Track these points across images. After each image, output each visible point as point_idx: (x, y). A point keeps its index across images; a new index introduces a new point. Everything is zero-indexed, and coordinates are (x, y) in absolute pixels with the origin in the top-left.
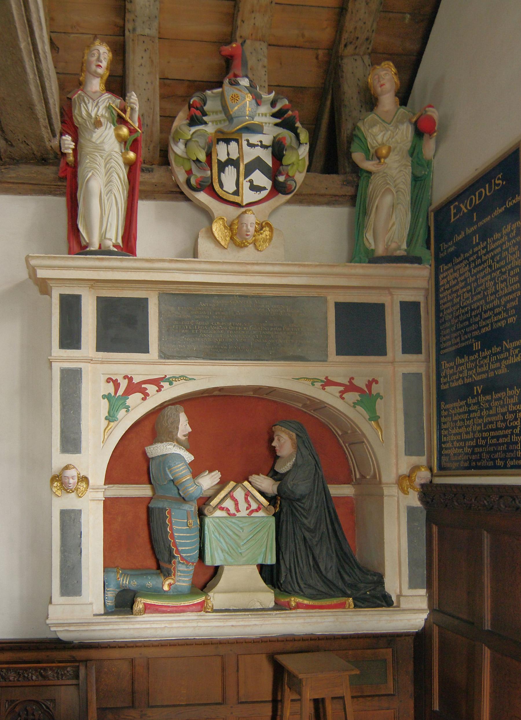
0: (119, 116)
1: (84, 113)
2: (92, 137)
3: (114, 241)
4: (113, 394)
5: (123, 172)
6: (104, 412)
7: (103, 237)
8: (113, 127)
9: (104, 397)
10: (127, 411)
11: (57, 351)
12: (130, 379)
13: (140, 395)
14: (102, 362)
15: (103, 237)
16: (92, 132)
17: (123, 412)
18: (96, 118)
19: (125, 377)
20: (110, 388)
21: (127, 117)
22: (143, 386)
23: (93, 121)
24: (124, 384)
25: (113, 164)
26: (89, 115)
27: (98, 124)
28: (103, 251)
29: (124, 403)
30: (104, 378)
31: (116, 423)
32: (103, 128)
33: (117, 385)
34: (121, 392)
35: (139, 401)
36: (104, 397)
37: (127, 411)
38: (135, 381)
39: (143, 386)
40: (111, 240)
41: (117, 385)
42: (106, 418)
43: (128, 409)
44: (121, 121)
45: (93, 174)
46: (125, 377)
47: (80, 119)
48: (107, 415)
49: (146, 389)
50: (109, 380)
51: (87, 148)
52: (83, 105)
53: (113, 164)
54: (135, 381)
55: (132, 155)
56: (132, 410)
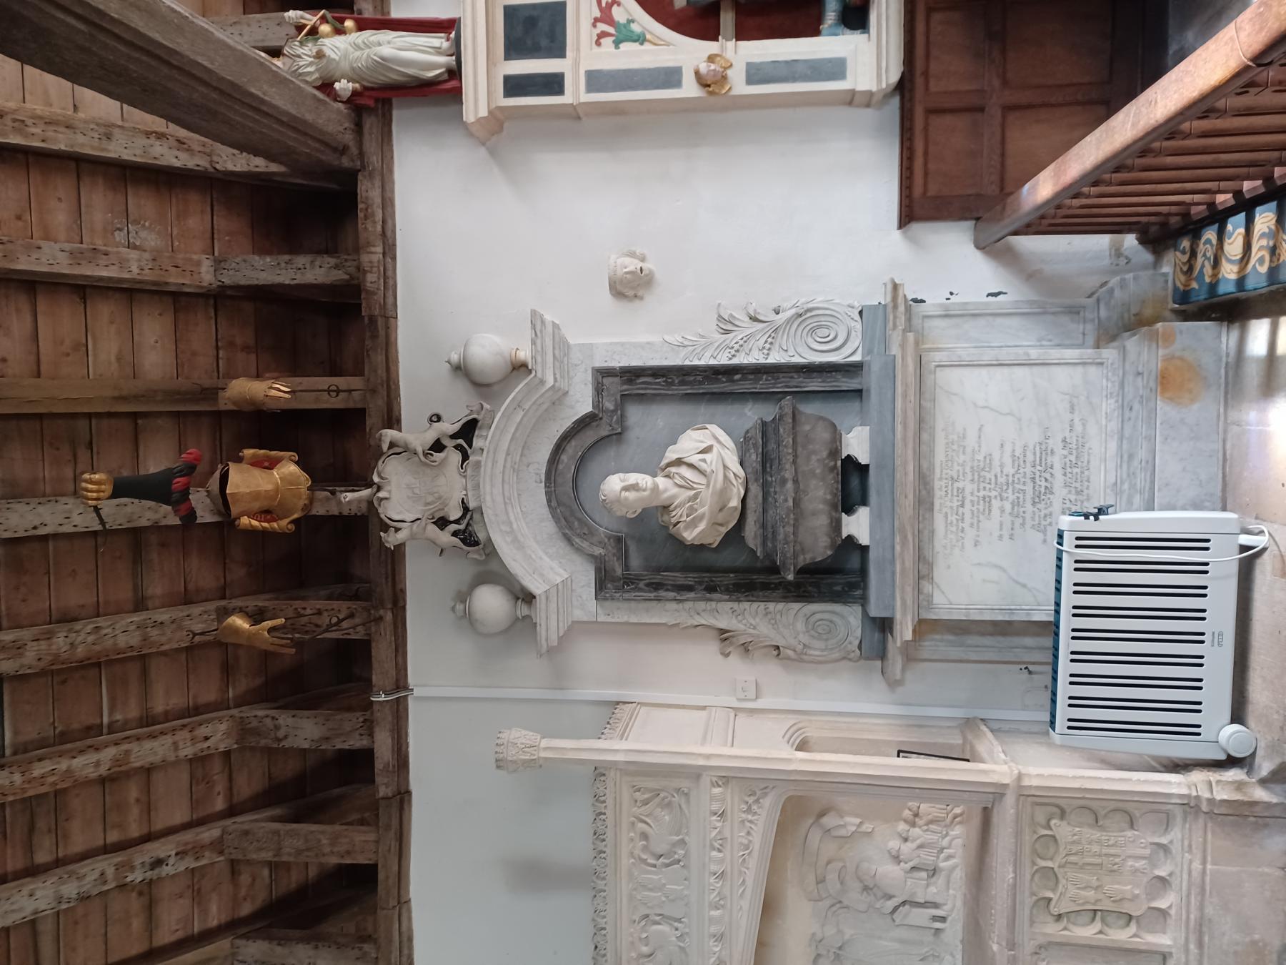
0: (307, 34)
1: (309, 69)
2: (334, 60)
3: (443, 40)
4: (614, 38)
5: (368, 35)
6: (634, 46)
7: (438, 51)
8: (321, 40)
9: (617, 47)
10: (633, 21)
11: (566, 99)
12: (596, 20)
13: (615, 9)
14: (578, 50)
15: (438, 51)
16: (331, 60)
17: (635, 28)
18: (314, 57)
19: (594, 26)
20: (607, 42)
21: (310, 24)
22: (604, 5)
23: (317, 61)
24: (603, 27)
25: (359, 41)
26: (311, 64)
27: (320, 55)
28: (457, 52)
29: (625, 26)
30: (596, 49)
31: (646, 33)
32: (325, 49)
33: (603, 35)
34: (611, 30)
35: (621, 9)
36: (617, 47)
37: (633, 21)
38: (597, 14)
39: (604, 5)
40: (442, 43)
41: (603, 35)
42: (642, 44)
43: (630, 21)
44: (314, 32)
45: (375, 55)
46: (594, 26)
47: (316, 75)
48: (637, 44)
49: (607, 3)
50: (598, 44)
51: (345, 66)
52: (300, 71)
53: (360, 41)
54: (597, 14)
55: (349, 24)
56: (631, 15)
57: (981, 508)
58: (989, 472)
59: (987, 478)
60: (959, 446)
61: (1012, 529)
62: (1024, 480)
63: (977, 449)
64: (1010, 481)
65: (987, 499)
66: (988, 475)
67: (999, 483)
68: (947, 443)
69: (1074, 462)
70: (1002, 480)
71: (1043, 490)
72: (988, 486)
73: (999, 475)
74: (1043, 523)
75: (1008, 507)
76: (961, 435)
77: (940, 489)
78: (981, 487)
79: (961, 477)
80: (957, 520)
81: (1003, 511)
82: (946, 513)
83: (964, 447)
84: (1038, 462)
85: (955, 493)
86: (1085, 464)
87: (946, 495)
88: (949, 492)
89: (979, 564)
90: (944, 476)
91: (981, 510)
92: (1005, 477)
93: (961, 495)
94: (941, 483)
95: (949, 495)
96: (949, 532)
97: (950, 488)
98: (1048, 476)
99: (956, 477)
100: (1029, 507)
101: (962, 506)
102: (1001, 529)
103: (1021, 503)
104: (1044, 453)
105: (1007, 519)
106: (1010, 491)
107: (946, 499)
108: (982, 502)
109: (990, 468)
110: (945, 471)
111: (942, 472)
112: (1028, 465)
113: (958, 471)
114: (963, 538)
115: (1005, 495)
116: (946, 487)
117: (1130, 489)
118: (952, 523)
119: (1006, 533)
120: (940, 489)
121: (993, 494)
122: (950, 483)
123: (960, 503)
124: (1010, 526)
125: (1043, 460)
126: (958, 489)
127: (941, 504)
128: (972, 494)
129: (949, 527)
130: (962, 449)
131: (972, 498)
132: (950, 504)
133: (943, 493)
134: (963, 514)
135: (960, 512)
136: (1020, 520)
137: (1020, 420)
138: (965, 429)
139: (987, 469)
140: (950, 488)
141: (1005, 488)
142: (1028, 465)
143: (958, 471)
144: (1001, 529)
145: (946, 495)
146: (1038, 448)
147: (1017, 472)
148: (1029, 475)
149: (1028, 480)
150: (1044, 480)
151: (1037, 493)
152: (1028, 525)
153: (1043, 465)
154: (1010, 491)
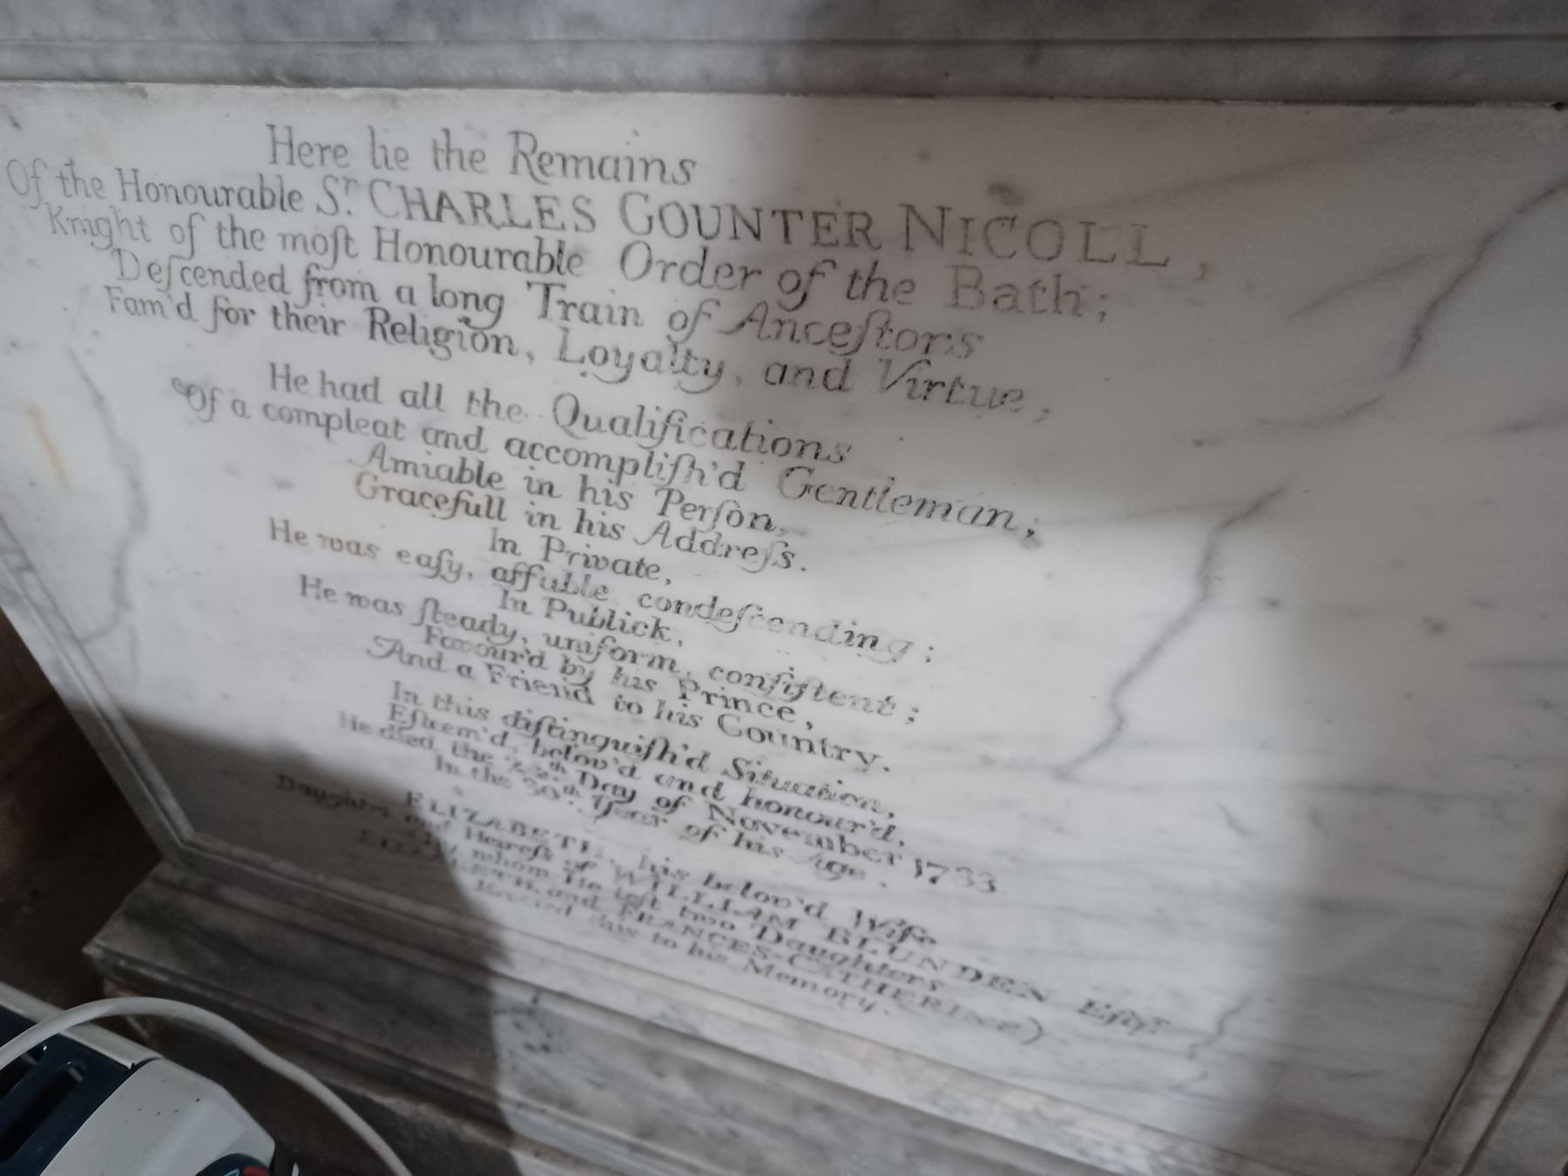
57: (412, 449)
58: (662, 530)
59: (614, 516)
60: (839, 334)
61: (355, 599)
62: (650, 709)
63: (826, 473)
64: (626, 641)
65: (479, 496)
66: (640, 518)
67: (600, 578)
68: (862, 233)
69: (787, 934)
70: (623, 594)
71: (609, 776)
72: (565, 509)
73: (655, 587)
74: (443, 743)
75: (476, 598)
76: (943, 368)
77: (445, 153)
78: (545, 471)
79: (583, 337)
80: (275, 281)
81: (438, 566)
82: (288, 200)
83: (836, 382)
84: (764, 793)
85: (458, 278)
86: (783, 967)
87: (415, 203)
88: (444, 233)
89: (99, 398)
90: (562, 187)
91: (397, 450)
92: (646, 616)
93: (448, 317)
94: (499, 153)
95: (419, 230)
96: (180, 214)
97: (482, 237)
98: (695, 812)
99: (578, 288)
100: (503, 700)
101: (383, 327)
102: (335, 544)
103: (512, 669)
104: (831, 833)
105: (412, 588)
106: (562, 626)
107: (390, 201)
108: (449, 458)
109: (690, 544)
110: (604, 195)
111: (597, 169)
112: (747, 749)
113: (628, 316)
114: (185, 308)
115: (535, 596)
116: (480, 205)
117: (664, 1096)
118: (250, 240)
119: (319, 562)
120: (445, 153)
121: (531, 545)
122: (522, 240)
123: (400, 313)
124: (367, 590)
125: (789, 822)
126: (493, 303)
127: (339, 151)
128: (484, 402)
129: (217, 215)
130: (822, 359)
131: (454, 400)
132: (365, 242)
133: (425, 177)
134: (332, 327)
135: (329, 305)
136: (414, 643)
137: (1062, 774)
138: (1003, 398)
139: (680, 527)
140: (482, 237)
141: (580, 605)
142: (747, 749)
143: (628, 316)
144: (335, 544)
145: (415, 203)
146: (853, 813)
147: (687, 687)
148: (678, 735)
149: (650, 728)
150: (672, 793)
151: (590, 750)
152: (413, 678)
153: (752, 813)
154: (562, 626)
